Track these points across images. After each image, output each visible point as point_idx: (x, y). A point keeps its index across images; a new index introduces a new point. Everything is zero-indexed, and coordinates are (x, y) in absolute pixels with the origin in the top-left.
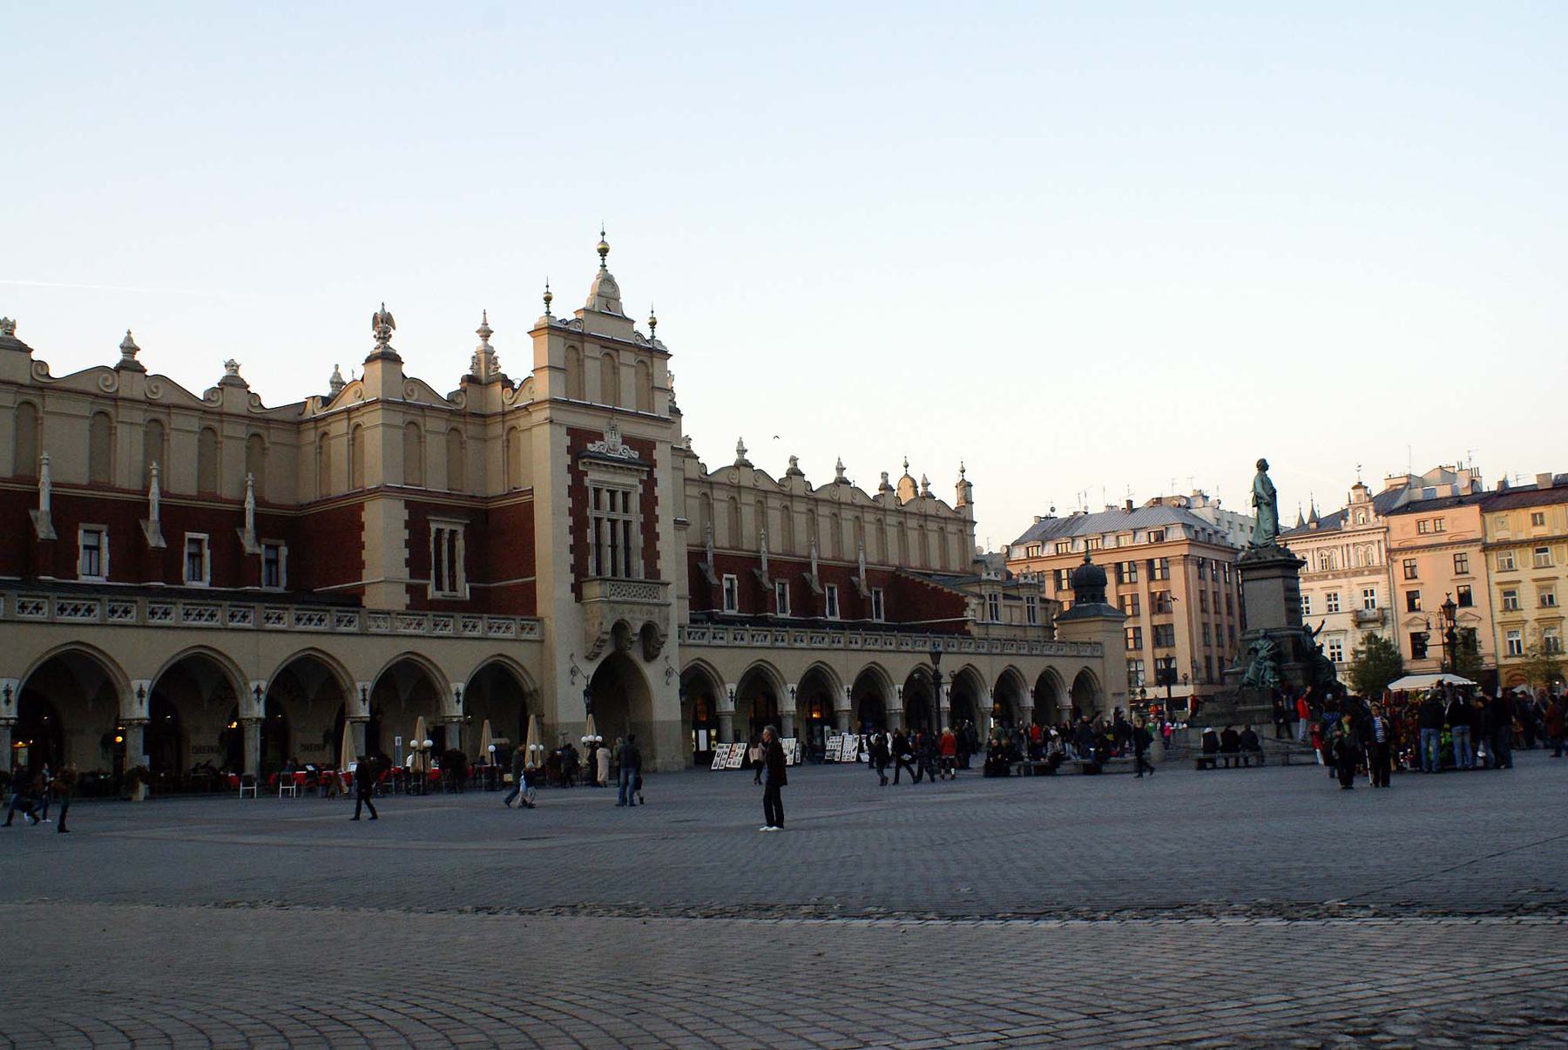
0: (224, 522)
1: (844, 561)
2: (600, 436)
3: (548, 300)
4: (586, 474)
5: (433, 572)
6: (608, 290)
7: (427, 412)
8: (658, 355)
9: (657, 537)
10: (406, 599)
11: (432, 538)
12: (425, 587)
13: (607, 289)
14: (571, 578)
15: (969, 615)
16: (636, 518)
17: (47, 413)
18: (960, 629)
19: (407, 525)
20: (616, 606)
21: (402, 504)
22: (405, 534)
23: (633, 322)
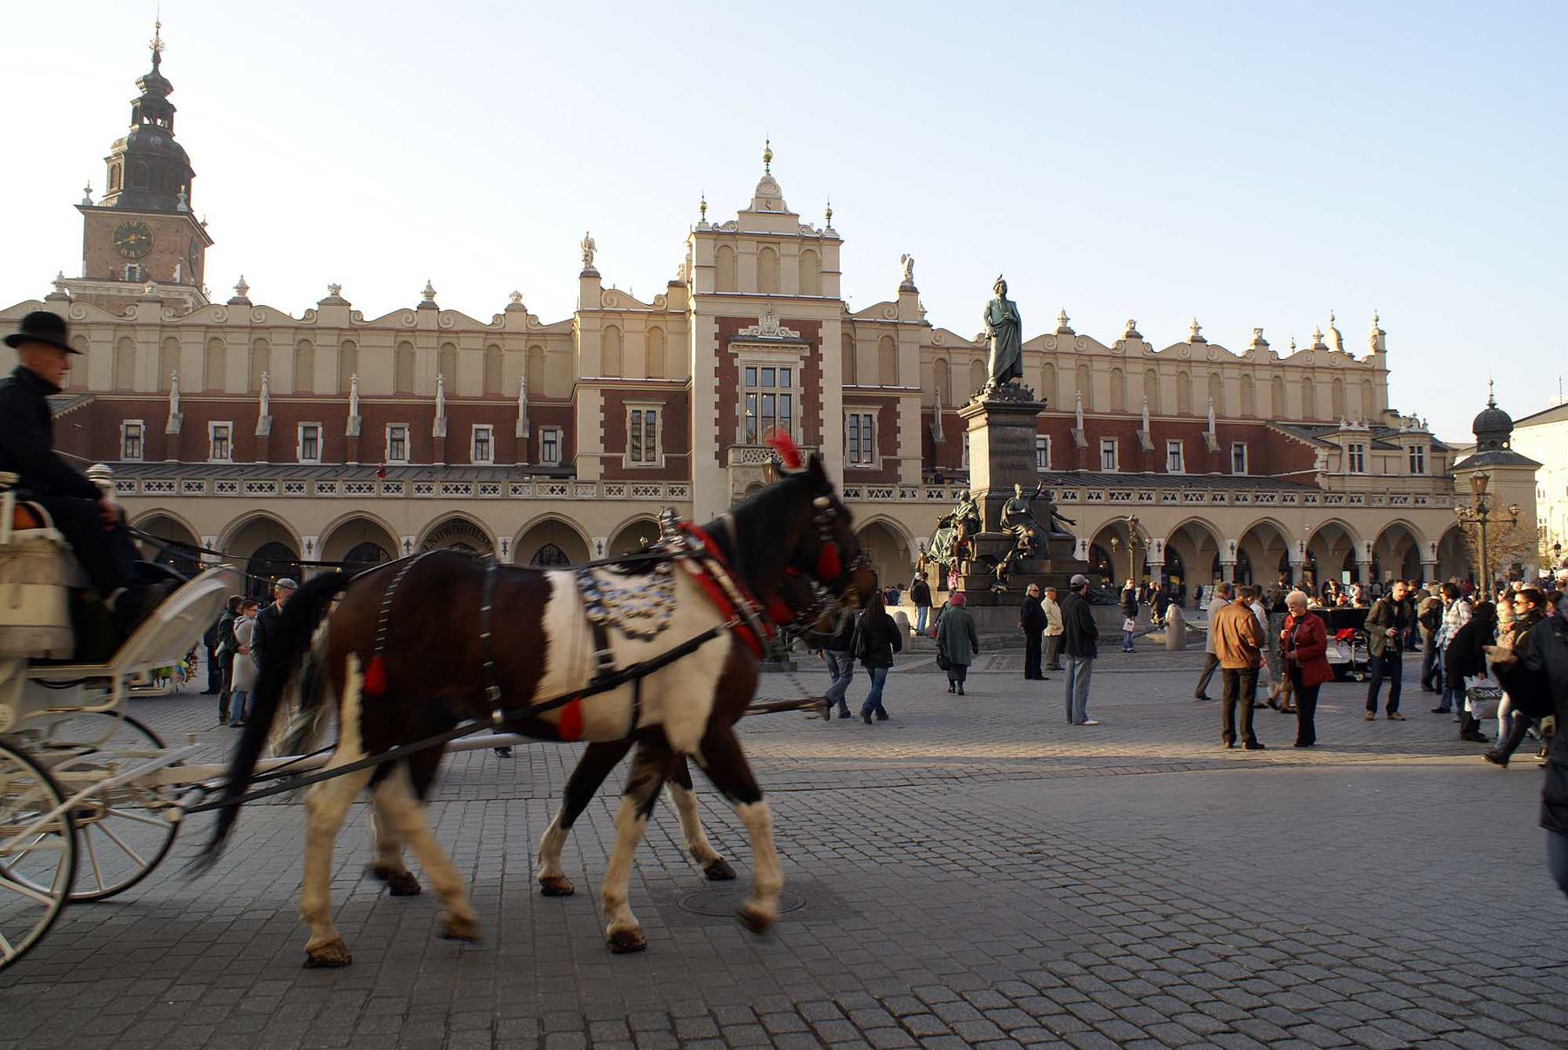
0: (502, 416)
1: (1192, 416)
2: (755, 322)
3: (703, 209)
4: (737, 356)
5: (628, 447)
6: (769, 191)
8: (826, 242)
9: (821, 406)
10: (602, 469)
11: (628, 419)
12: (621, 458)
13: (768, 193)
14: (717, 447)
15: (1319, 466)
16: (797, 390)
17: (275, 345)
18: (1308, 483)
19: (603, 409)
20: (750, 470)
22: (602, 417)
23: (798, 216)
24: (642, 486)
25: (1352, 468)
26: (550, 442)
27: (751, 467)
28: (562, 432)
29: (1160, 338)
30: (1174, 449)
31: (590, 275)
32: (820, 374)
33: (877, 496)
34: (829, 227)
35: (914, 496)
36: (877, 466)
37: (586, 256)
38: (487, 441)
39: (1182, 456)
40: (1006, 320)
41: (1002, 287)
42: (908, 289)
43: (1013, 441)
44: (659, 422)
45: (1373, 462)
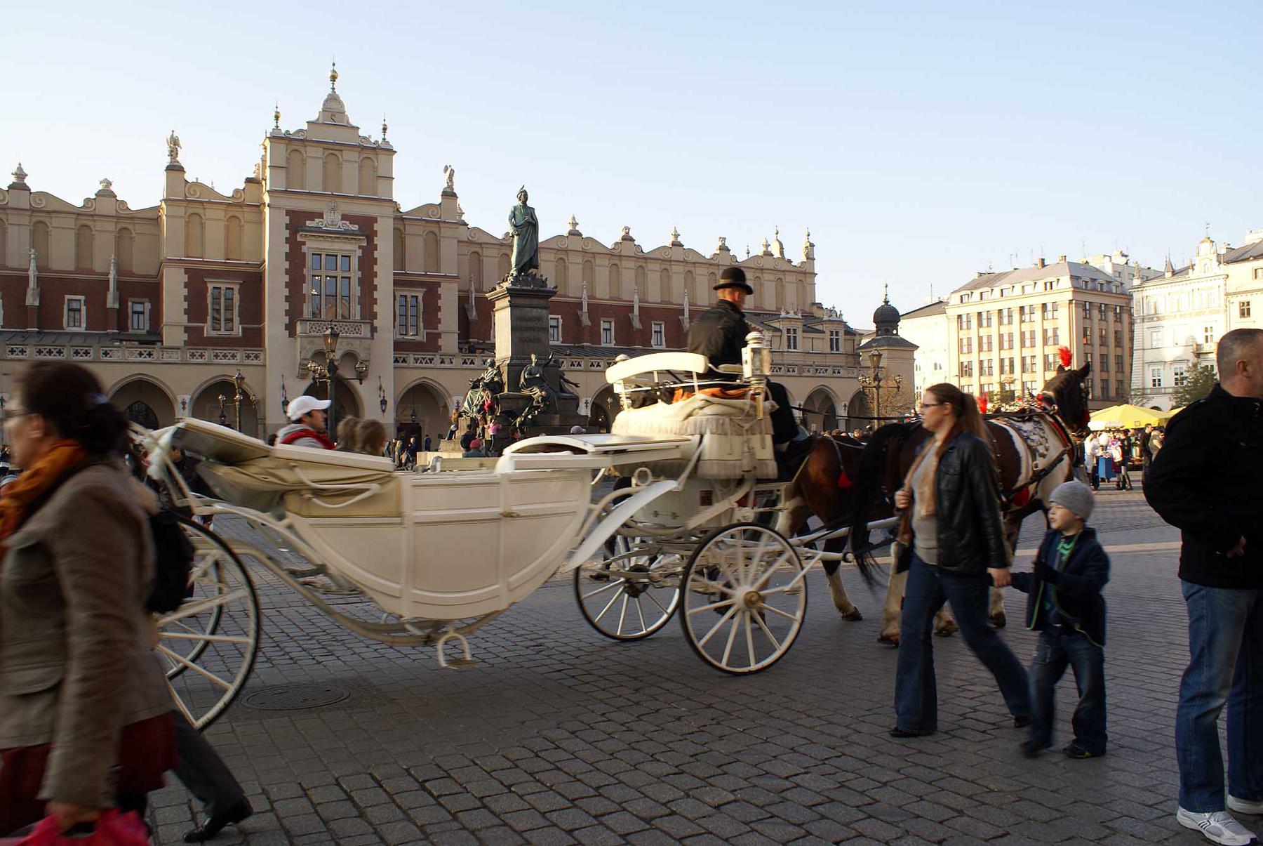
0: (95, 290)
1: (672, 304)
3: (277, 118)
4: (304, 243)
5: (209, 318)
6: (334, 106)
7: (207, 206)
8: (382, 152)
9: (375, 288)
10: (185, 337)
12: (202, 328)
13: (333, 107)
14: (286, 320)
16: (355, 274)
19: (186, 285)
20: (316, 339)
21: (183, 271)
22: (185, 292)
23: (358, 128)
24: (221, 352)
25: (789, 346)
26: (139, 313)
27: (314, 337)
28: (149, 305)
29: (649, 242)
30: (657, 329)
31: (175, 169)
32: (375, 261)
33: (421, 362)
34: (384, 139)
35: (452, 363)
36: (422, 337)
37: (172, 151)
38: (79, 310)
39: (663, 334)
40: (526, 222)
41: (524, 196)
42: (449, 194)
43: (531, 319)
44: (236, 297)
45: (804, 341)
